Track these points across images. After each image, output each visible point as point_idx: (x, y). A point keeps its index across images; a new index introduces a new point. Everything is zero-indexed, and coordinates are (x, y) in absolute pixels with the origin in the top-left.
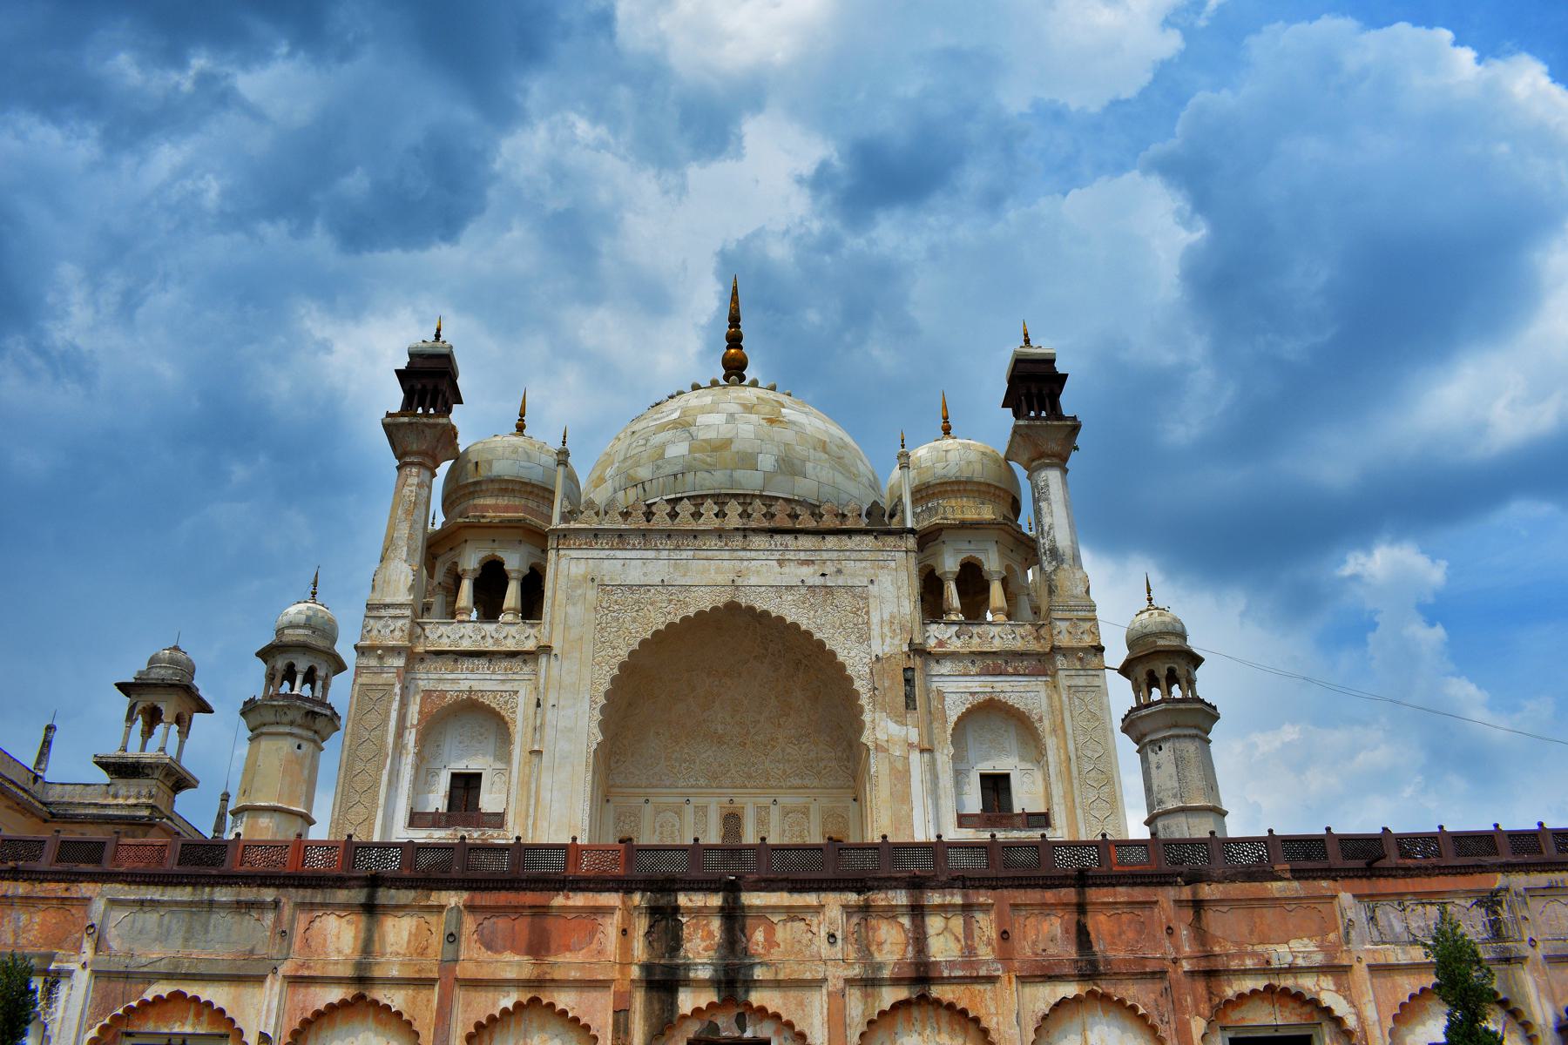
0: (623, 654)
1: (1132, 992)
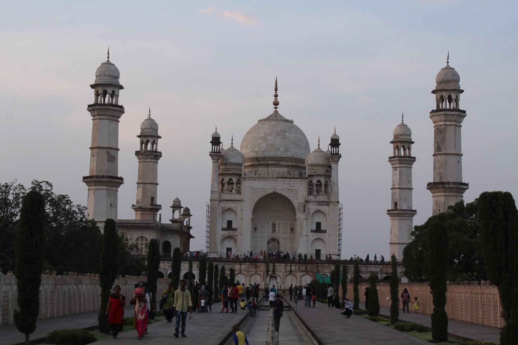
0: (256, 201)
1: (310, 273)
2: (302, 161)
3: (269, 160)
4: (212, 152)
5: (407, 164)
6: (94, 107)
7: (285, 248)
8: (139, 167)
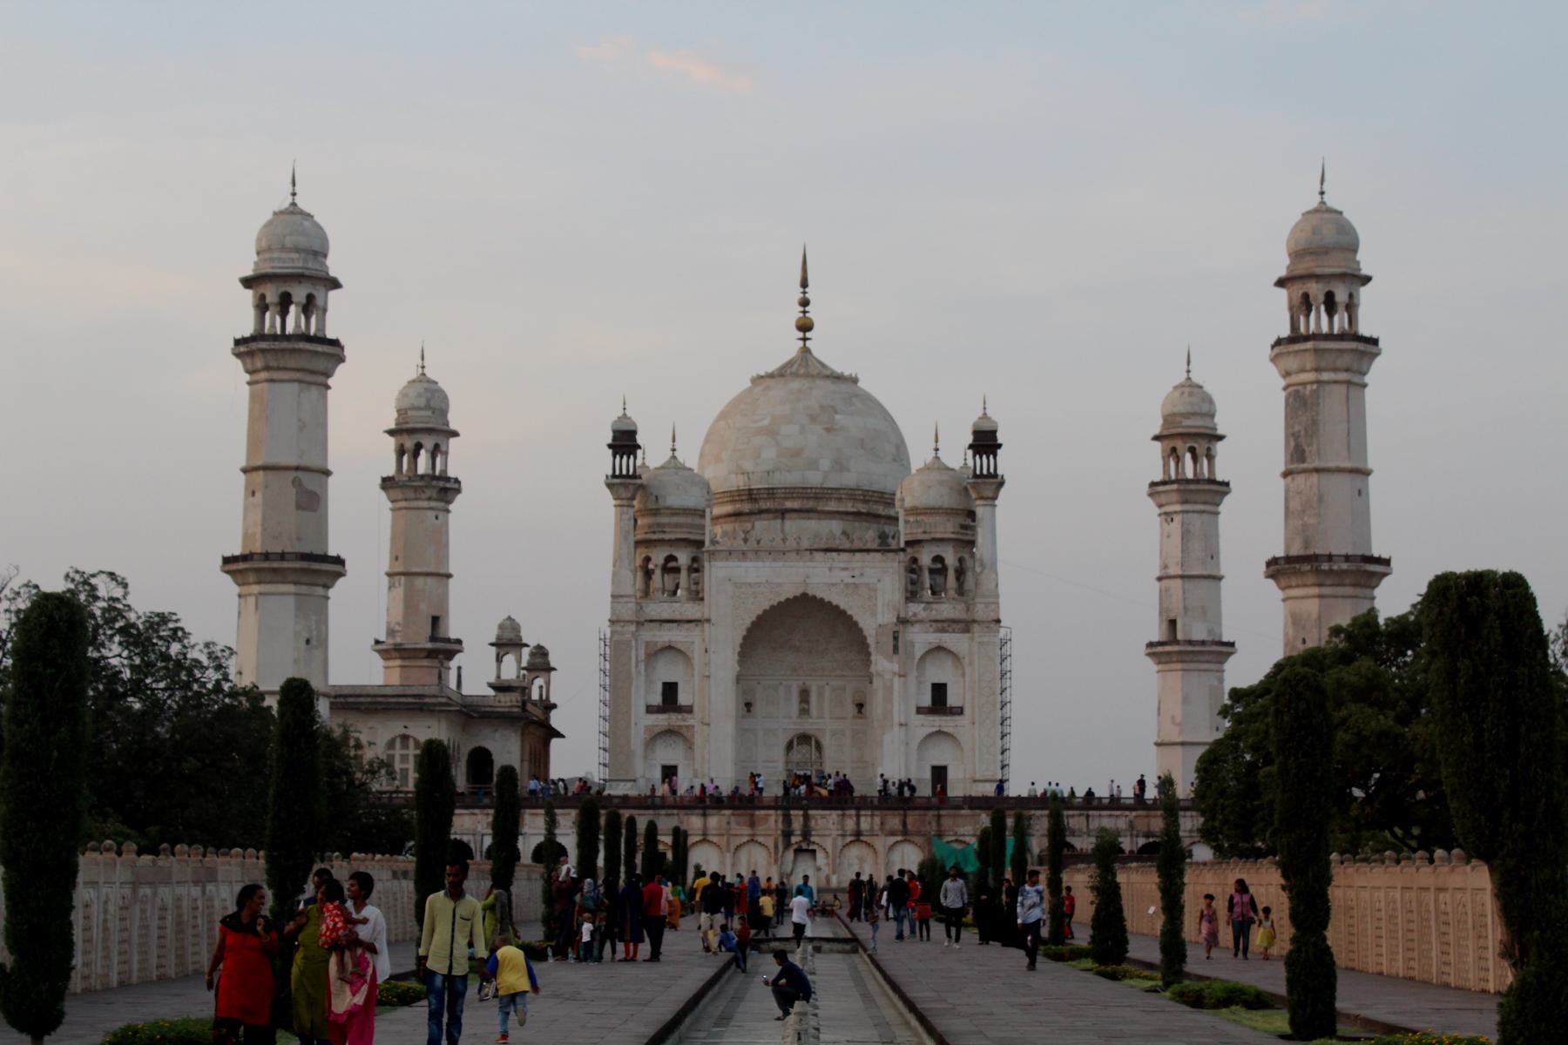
0: (748, 623)
2: (887, 499)
3: (786, 499)
4: (614, 476)
5: (1205, 503)
6: (254, 346)
7: (837, 761)
8: (394, 526)
